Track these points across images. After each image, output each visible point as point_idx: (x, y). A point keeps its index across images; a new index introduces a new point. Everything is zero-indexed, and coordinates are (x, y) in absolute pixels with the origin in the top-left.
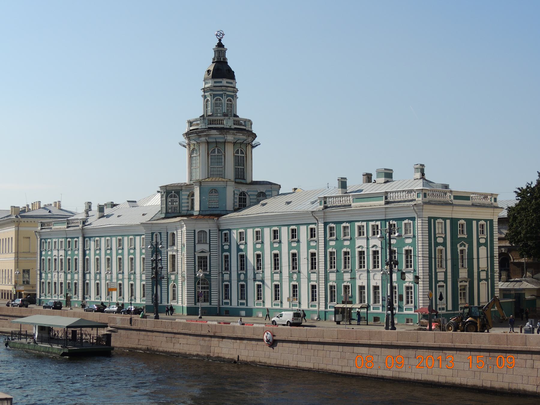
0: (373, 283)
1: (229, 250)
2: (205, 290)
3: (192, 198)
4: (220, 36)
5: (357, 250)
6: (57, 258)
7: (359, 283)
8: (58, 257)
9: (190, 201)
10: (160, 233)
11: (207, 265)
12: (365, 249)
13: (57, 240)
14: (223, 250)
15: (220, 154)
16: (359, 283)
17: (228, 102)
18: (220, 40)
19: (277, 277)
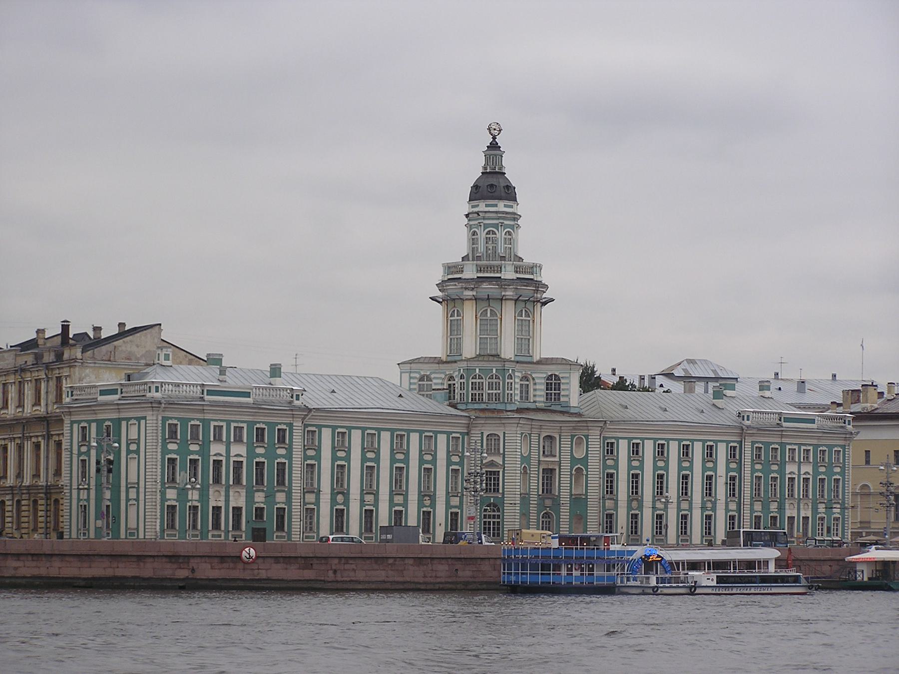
0: (802, 514)
1: (616, 466)
2: (494, 520)
3: (522, 382)
4: (494, 131)
5: (788, 476)
6: (223, 459)
7: (788, 513)
8: (228, 457)
9: (518, 386)
10: (530, 434)
11: (498, 484)
12: (796, 476)
13: (224, 424)
14: (605, 466)
15: (527, 318)
16: (788, 513)
17: (506, 237)
18: (494, 138)
19: (685, 505)
